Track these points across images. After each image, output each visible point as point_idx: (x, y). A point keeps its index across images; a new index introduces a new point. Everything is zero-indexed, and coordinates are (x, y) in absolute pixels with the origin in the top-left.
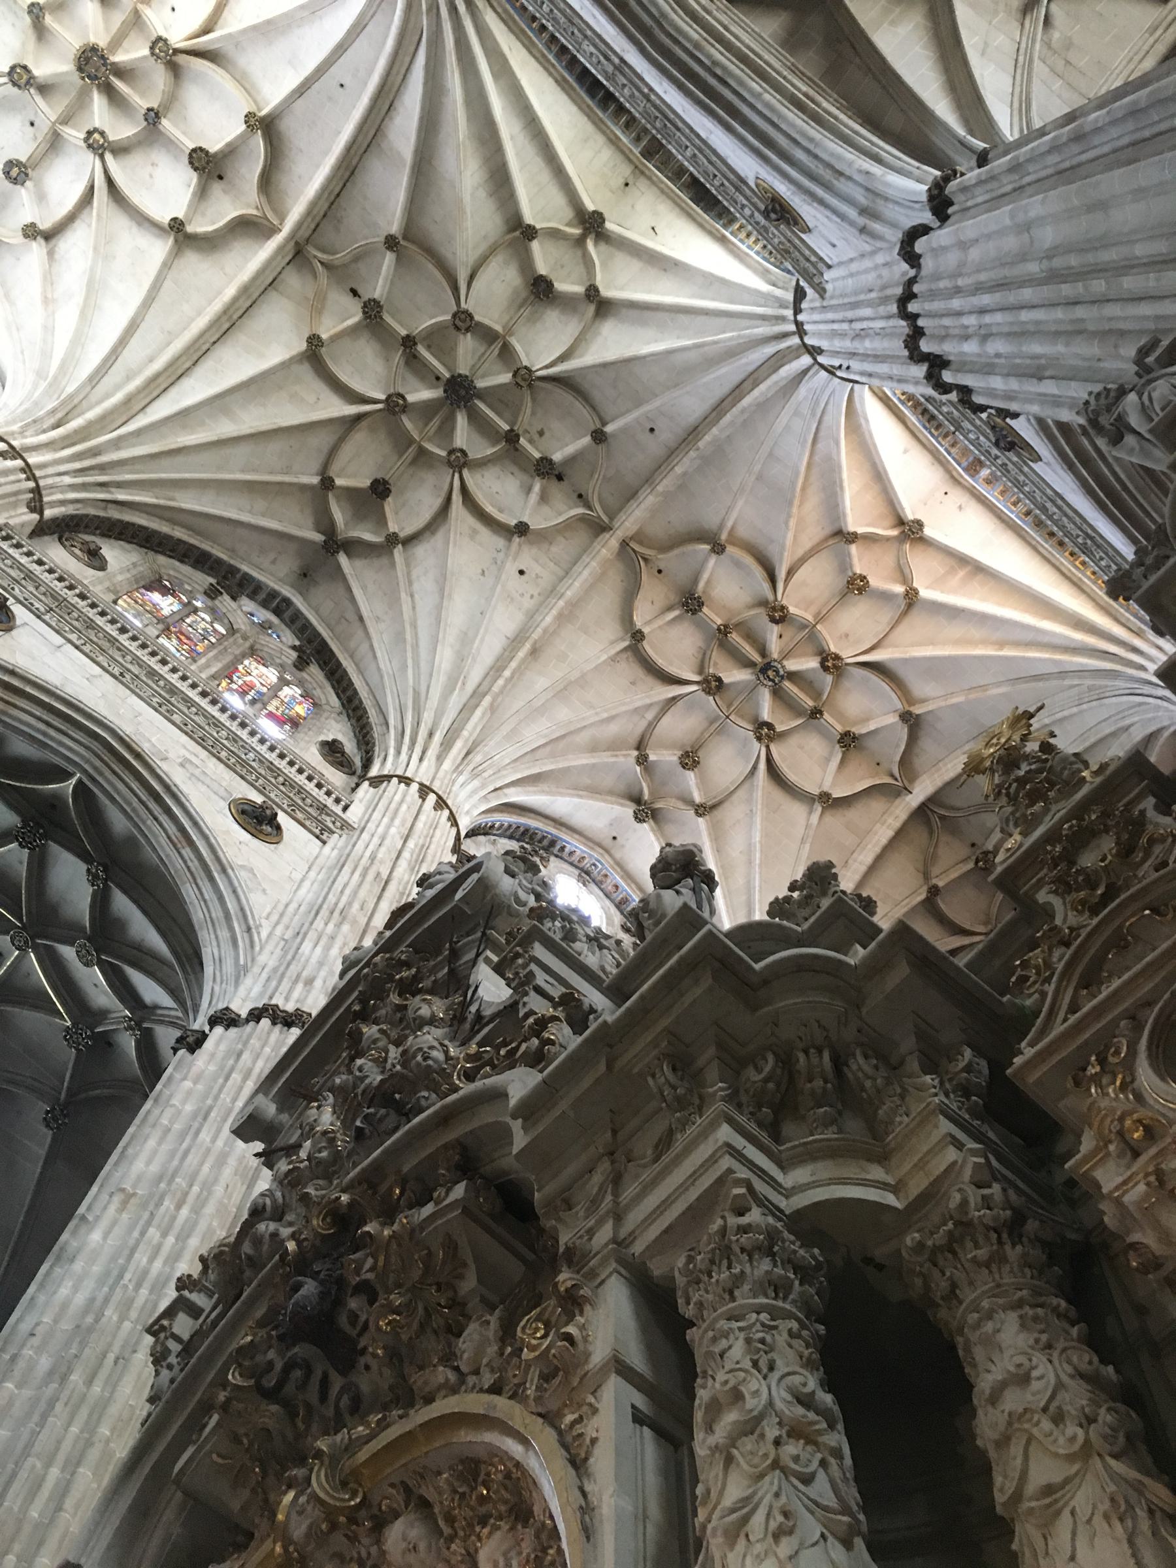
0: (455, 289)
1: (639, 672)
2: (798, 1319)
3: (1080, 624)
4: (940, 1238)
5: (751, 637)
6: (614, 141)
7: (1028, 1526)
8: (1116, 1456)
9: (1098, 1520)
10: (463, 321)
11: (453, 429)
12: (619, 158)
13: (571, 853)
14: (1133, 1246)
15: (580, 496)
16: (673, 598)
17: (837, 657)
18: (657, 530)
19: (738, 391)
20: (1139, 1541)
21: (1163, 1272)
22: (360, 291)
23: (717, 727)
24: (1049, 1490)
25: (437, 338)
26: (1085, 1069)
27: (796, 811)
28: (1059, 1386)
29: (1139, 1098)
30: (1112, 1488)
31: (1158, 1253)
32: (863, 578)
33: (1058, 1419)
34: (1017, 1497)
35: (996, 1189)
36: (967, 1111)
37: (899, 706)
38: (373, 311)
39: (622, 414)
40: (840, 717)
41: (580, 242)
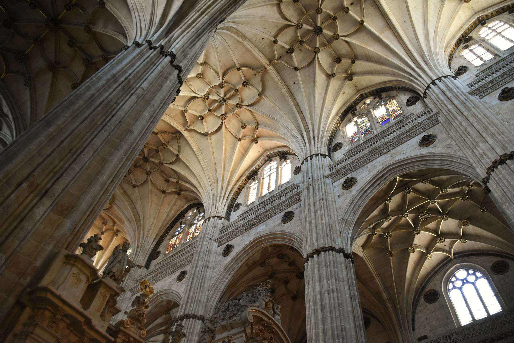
1: (228, 67)
3: (229, 182)
5: (232, 97)
6: (367, 87)
10: (336, 37)
11: (307, 24)
12: (363, 87)
15: (281, 57)
16: (247, 77)
17: (225, 119)
18: (267, 77)
19: (301, 112)
22: (352, 6)
25: (333, 27)
32: (245, 128)
37: (210, 132)
39: (301, 76)
40: (207, 115)
41: (346, 72)
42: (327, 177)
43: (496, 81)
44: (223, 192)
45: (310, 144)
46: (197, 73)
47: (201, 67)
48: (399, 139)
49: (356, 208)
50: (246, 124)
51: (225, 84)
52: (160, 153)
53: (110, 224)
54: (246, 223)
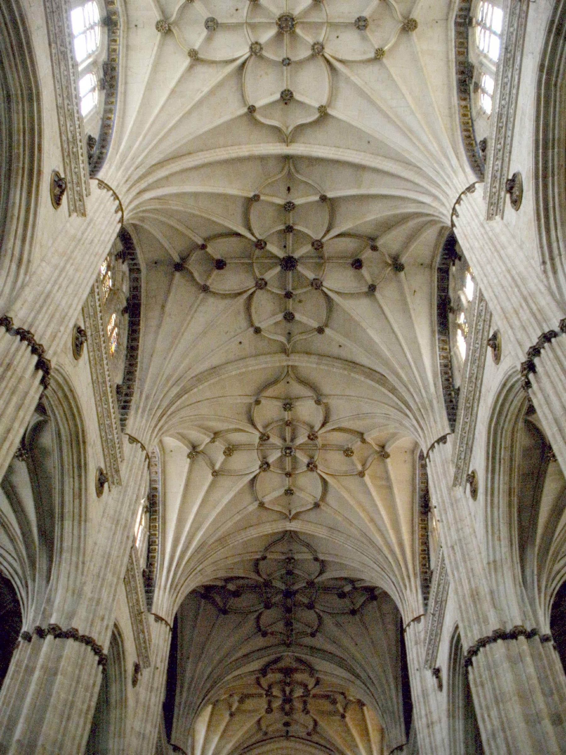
0: (328, 231)
10: (318, 245)
11: (270, 268)
15: (289, 333)
17: (316, 467)
22: (292, 190)
23: (247, 446)
27: (248, 498)
32: (352, 452)
37: (319, 498)
38: (289, 207)
42: (454, 485)
43: (497, 171)
44: (404, 569)
45: (422, 429)
46: (222, 453)
47: (217, 443)
48: (477, 361)
49: (496, 528)
50: (350, 446)
51: (268, 429)
52: (296, 571)
53: (340, 698)
54: (433, 619)
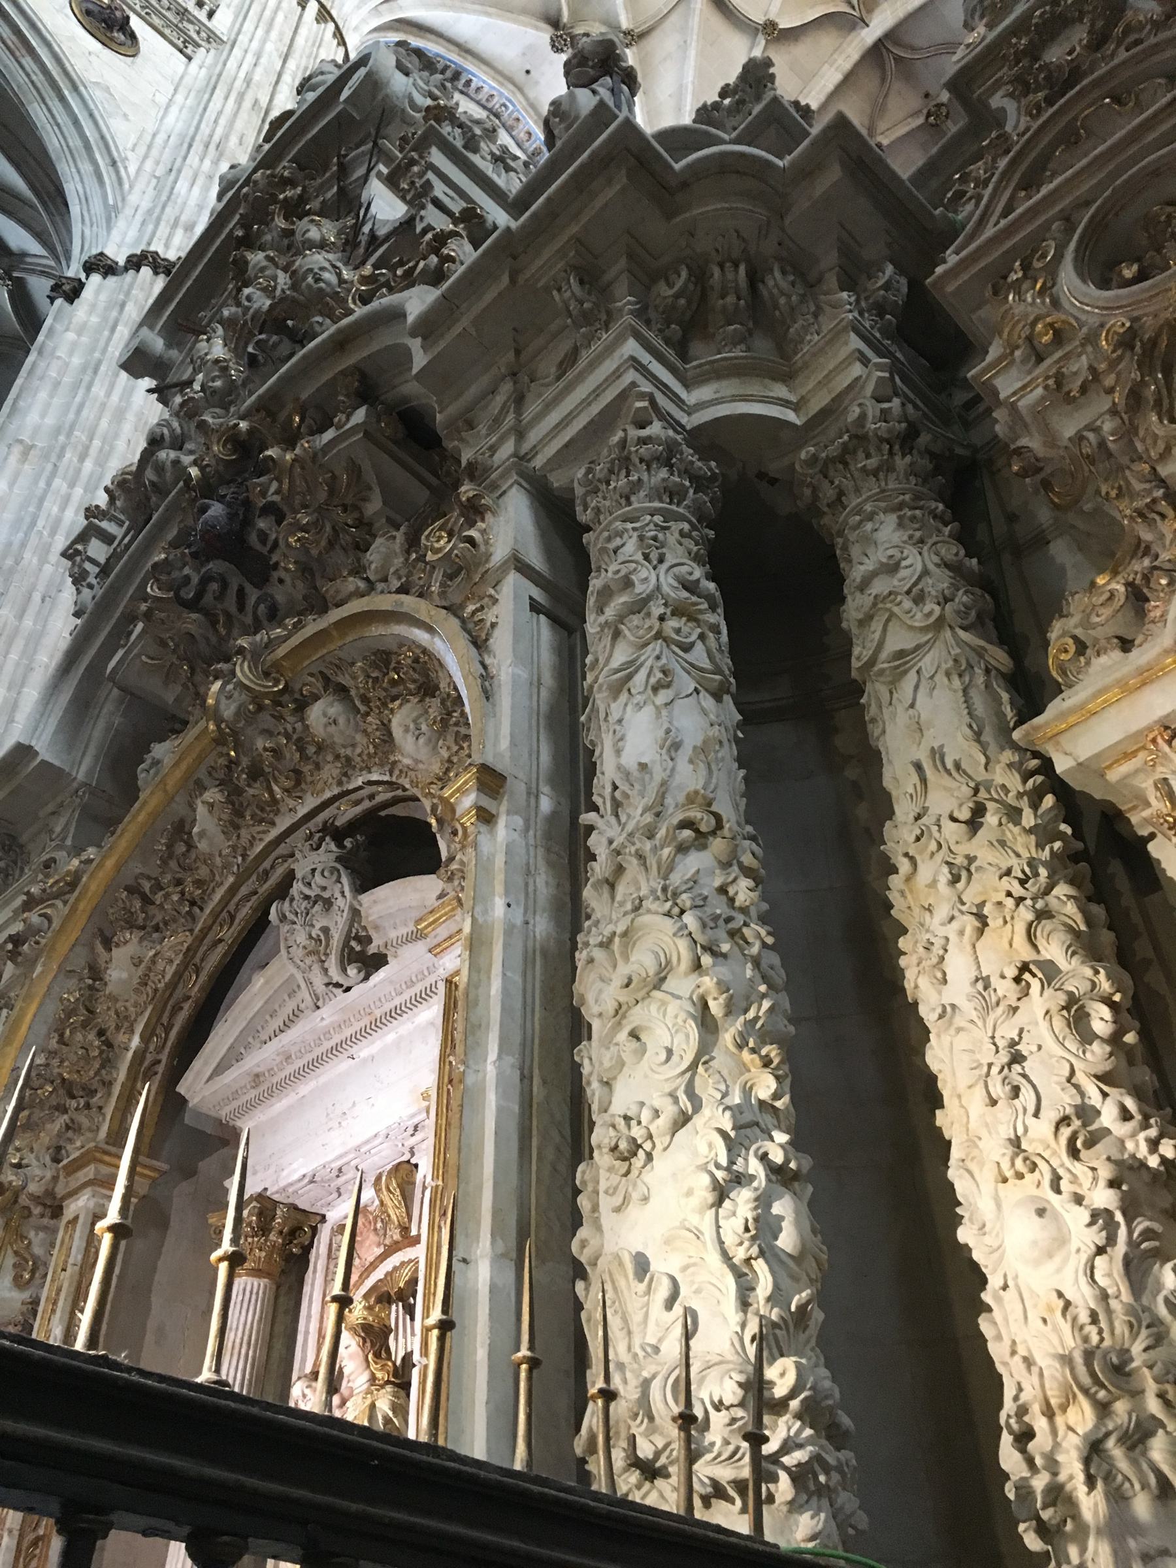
2: (690, 522)
4: (833, 450)
7: (878, 686)
8: (964, 629)
9: (941, 678)
13: (478, 89)
14: (1018, 452)
20: (973, 693)
21: (1042, 475)
24: (901, 654)
26: (1005, 277)
28: (925, 572)
29: (1056, 303)
30: (958, 651)
31: (1040, 455)
33: (919, 599)
34: (872, 662)
35: (896, 402)
36: (879, 330)
